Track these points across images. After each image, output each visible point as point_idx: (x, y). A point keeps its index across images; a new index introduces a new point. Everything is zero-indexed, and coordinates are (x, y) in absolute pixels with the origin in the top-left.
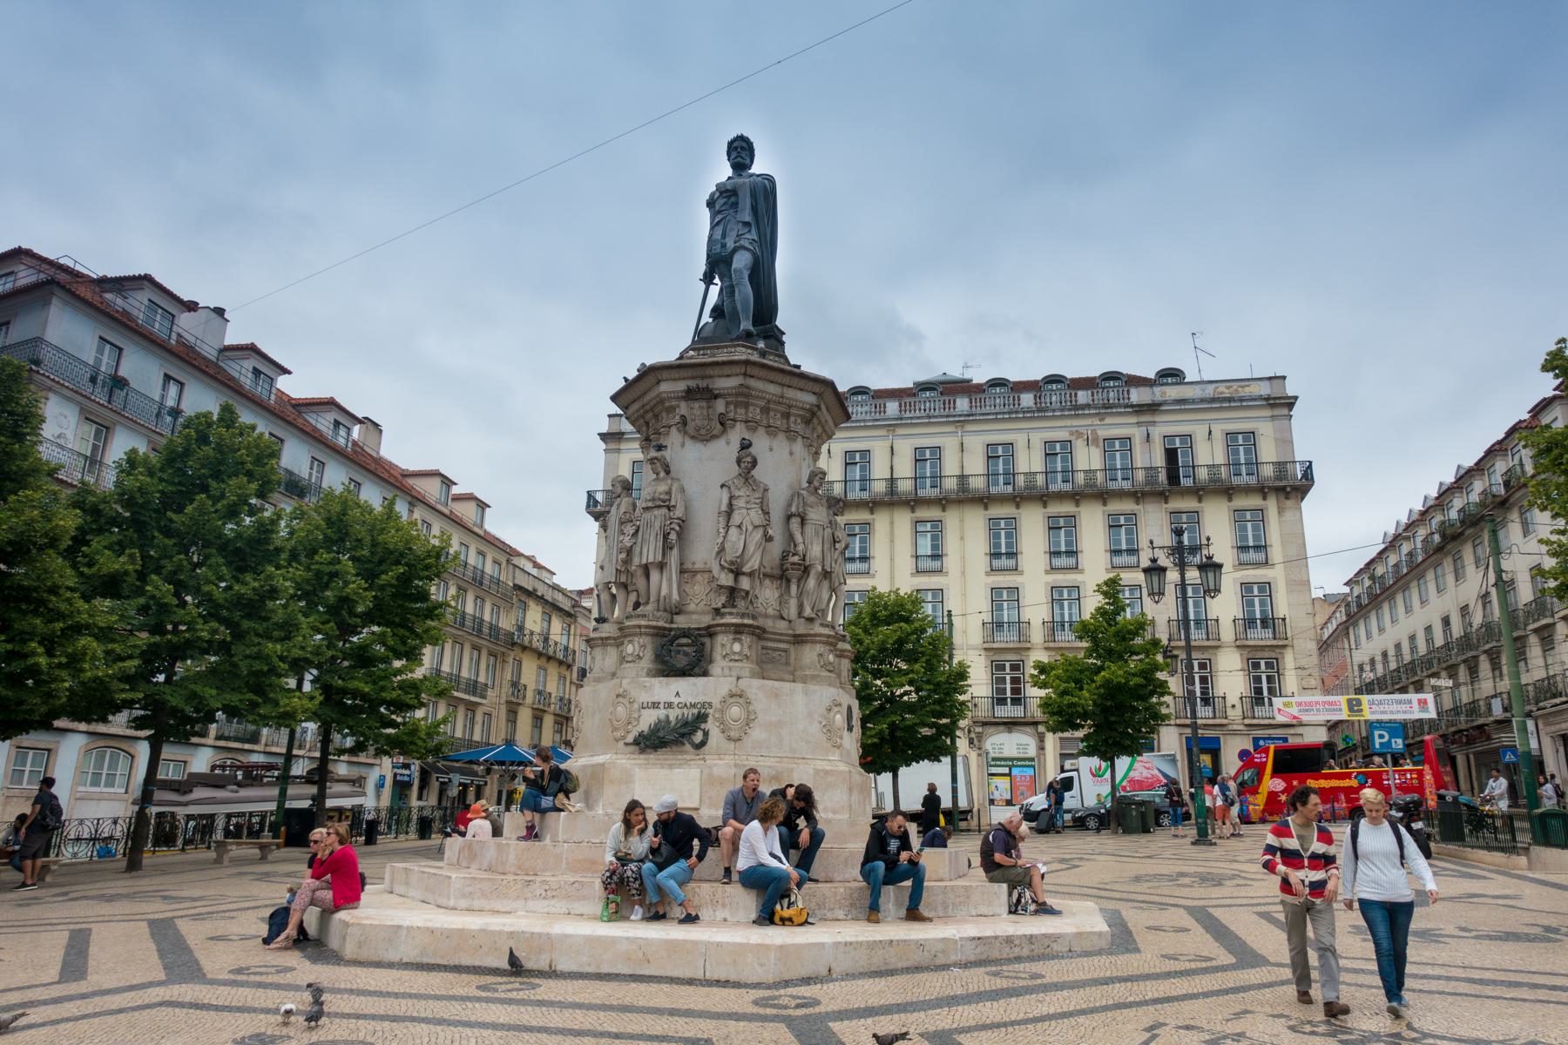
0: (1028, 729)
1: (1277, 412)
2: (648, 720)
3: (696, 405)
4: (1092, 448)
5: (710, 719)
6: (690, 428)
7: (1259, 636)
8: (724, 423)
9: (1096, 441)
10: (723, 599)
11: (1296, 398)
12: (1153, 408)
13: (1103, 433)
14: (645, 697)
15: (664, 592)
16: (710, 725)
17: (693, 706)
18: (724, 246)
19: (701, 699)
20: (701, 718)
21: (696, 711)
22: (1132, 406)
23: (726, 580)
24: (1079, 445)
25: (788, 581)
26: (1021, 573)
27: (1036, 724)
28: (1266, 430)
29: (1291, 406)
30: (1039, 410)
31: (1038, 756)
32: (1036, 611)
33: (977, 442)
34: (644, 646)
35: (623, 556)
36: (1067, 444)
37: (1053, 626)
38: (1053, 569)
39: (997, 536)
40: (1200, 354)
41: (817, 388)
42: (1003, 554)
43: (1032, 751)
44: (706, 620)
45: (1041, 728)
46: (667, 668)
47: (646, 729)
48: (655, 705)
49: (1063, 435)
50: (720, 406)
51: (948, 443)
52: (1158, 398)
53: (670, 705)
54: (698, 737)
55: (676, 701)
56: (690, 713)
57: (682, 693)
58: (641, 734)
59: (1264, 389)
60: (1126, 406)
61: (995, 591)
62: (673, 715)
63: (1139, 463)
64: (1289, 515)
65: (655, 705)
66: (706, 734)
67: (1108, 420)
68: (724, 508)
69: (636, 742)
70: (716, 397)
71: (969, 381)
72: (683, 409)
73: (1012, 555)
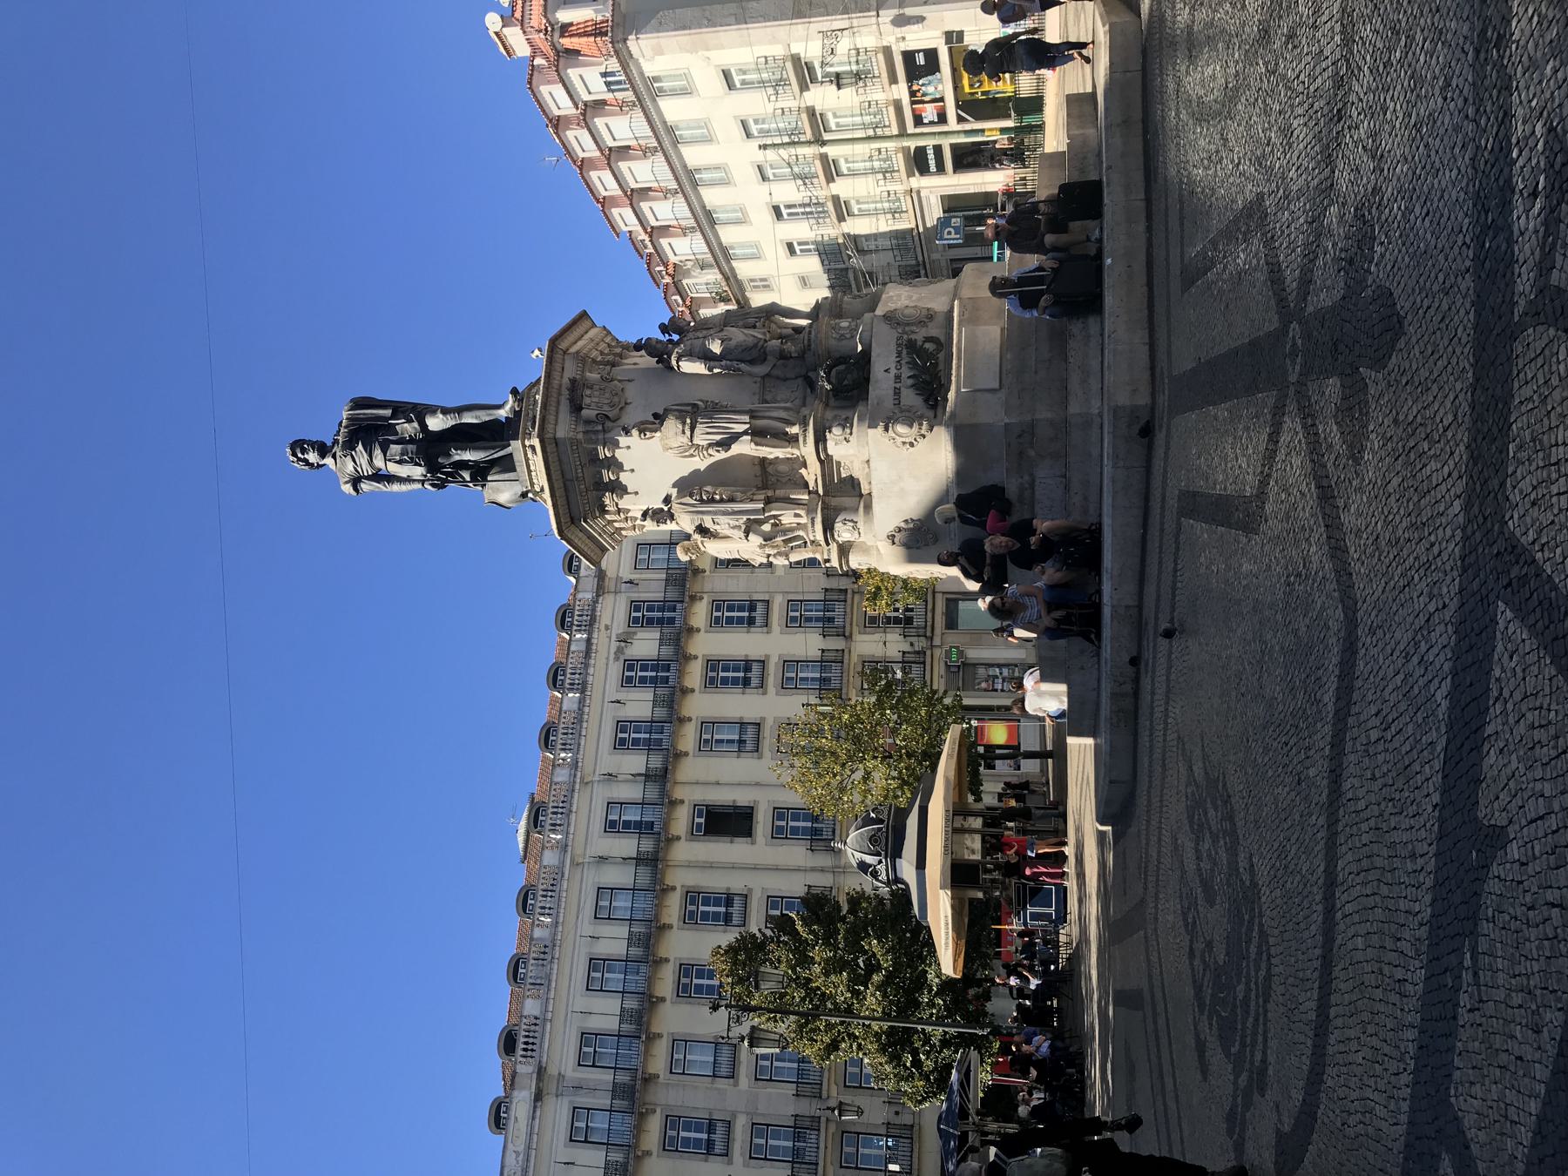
2: (911, 398)
3: (587, 400)
5: (913, 337)
14: (889, 402)
16: (919, 335)
17: (899, 354)
18: (412, 441)
19: (893, 347)
20: (911, 346)
26: (763, 719)
30: (583, 692)
36: (630, 665)
38: (762, 685)
39: (705, 916)
49: (615, 670)
53: (898, 378)
54: (929, 346)
55: (893, 371)
58: (926, 401)
60: (595, 602)
62: (906, 372)
63: (660, 596)
65: (897, 392)
66: (928, 339)
73: (752, 606)
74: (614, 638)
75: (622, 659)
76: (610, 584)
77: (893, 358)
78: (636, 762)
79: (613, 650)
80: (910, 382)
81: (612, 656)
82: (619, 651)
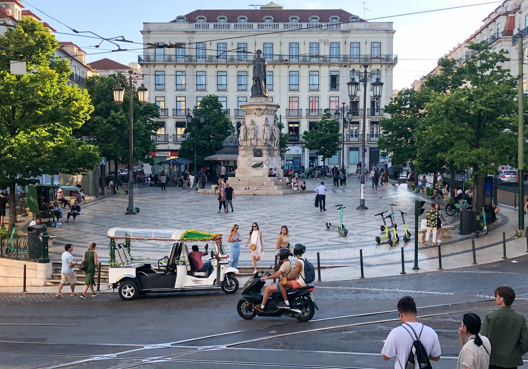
0: (299, 145)
1: (390, 35)
2: (254, 163)
4: (326, 46)
9: (327, 43)
11: (395, 31)
12: (348, 31)
13: (331, 40)
20: (262, 163)
22: (341, 31)
23: (265, 142)
24: (322, 45)
26: (300, 91)
27: (302, 143)
28: (385, 43)
29: (394, 33)
31: (302, 154)
32: (304, 105)
37: (310, 111)
40: (366, 10)
43: (300, 153)
45: (304, 145)
46: (256, 155)
49: (316, 40)
50: (262, 111)
57: (259, 159)
59: (386, 27)
64: (389, 72)
67: (333, 35)
71: (281, 8)
72: (255, 111)
74: (326, 39)
75: (320, 42)
76: (345, 35)
78: (285, 52)
79: (323, 39)
82: (322, 41)
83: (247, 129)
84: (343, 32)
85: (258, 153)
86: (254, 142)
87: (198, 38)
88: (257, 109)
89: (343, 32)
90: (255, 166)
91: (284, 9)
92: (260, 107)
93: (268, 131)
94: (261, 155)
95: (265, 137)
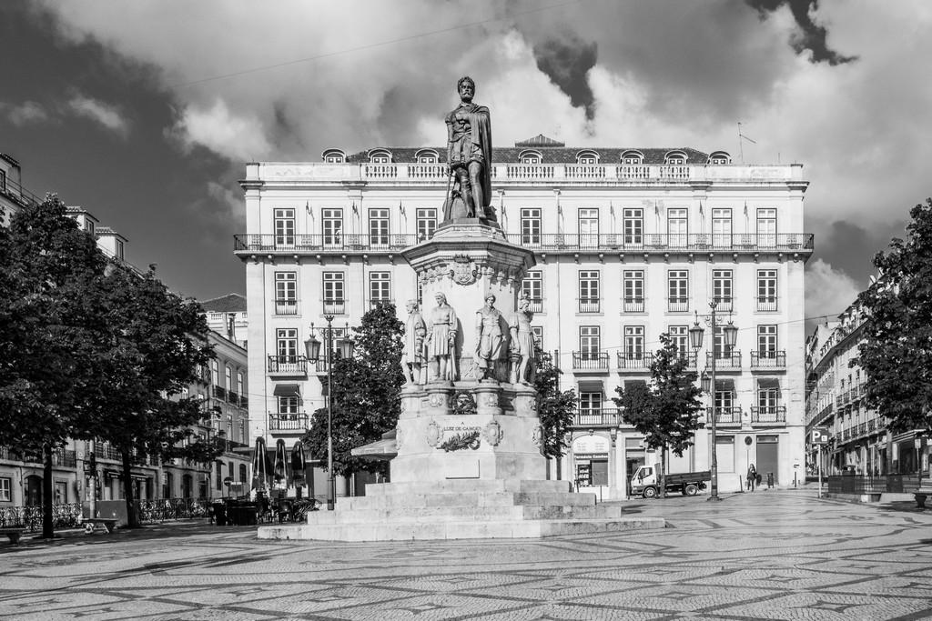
6: (456, 277)
7: (767, 364)
8: (476, 275)
10: (483, 374)
12: (706, 186)
14: (445, 425)
15: (448, 369)
20: (476, 434)
21: (473, 431)
23: (483, 364)
25: (511, 363)
33: (571, 202)
34: (441, 399)
35: (418, 347)
41: (524, 254)
42: (589, 293)
44: (474, 385)
47: (448, 442)
48: (451, 429)
50: (473, 266)
51: (546, 202)
52: (710, 177)
53: (459, 429)
54: (475, 443)
55: (462, 426)
56: (470, 432)
57: (465, 423)
61: (584, 330)
65: (451, 429)
66: (479, 442)
67: (672, 193)
68: (479, 325)
69: (443, 447)
70: (471, 261)
71: (563, 145)
72: (452, 266)
77: (469, 426)
80: (456, 435)
81: (646, 199)
82: (650, 203)
83: (425, 328)
84: (696, 186)
85: (459, 402)
86: (449, 366)
87: (374, 200)
88: (455, 259)
89: (696, 186)
90: (452, 446)
91: (567, 146)
92: (465, 253)
93: (492, 329)
94: (472, 408)
95: (485, 351)
